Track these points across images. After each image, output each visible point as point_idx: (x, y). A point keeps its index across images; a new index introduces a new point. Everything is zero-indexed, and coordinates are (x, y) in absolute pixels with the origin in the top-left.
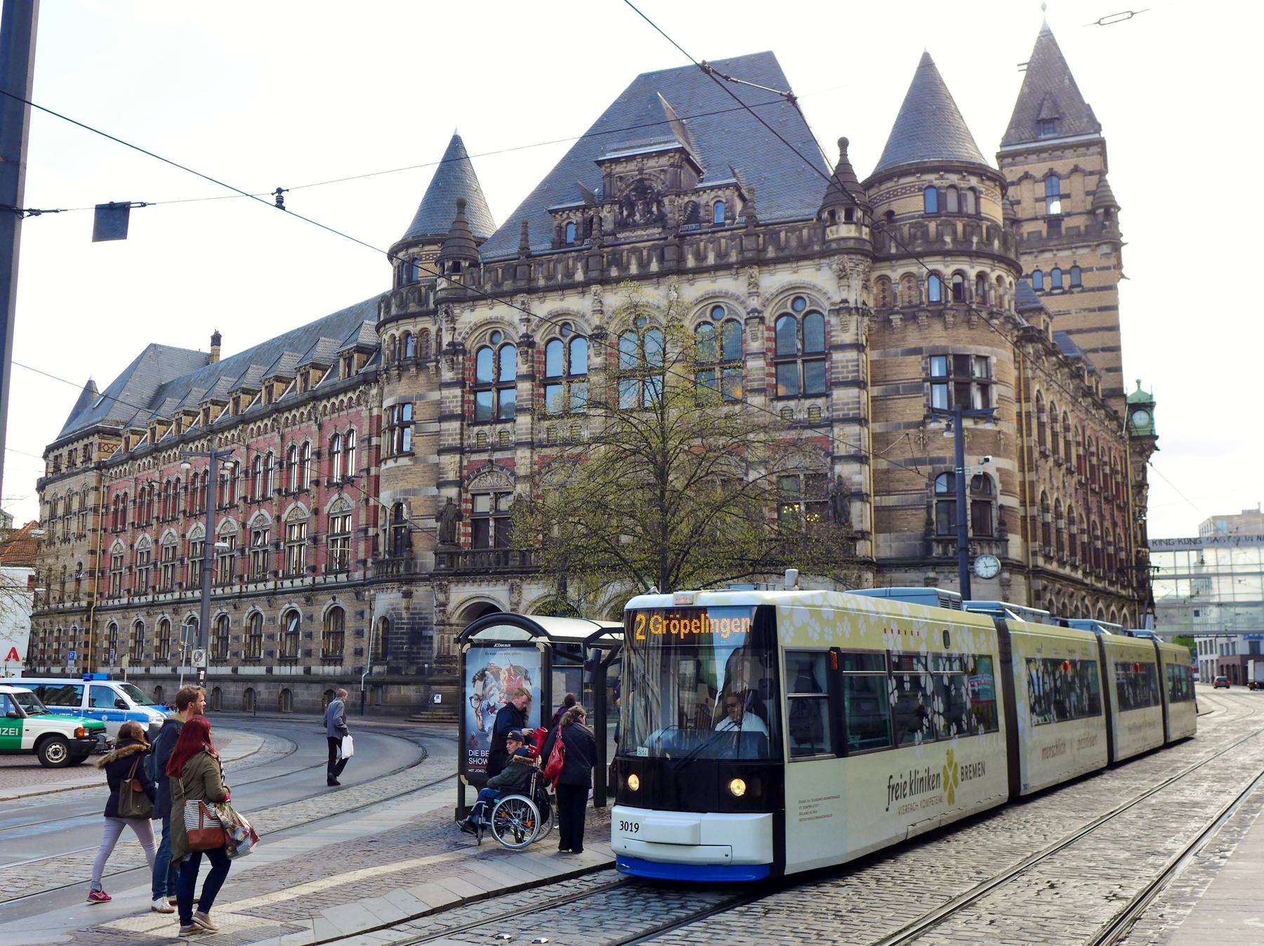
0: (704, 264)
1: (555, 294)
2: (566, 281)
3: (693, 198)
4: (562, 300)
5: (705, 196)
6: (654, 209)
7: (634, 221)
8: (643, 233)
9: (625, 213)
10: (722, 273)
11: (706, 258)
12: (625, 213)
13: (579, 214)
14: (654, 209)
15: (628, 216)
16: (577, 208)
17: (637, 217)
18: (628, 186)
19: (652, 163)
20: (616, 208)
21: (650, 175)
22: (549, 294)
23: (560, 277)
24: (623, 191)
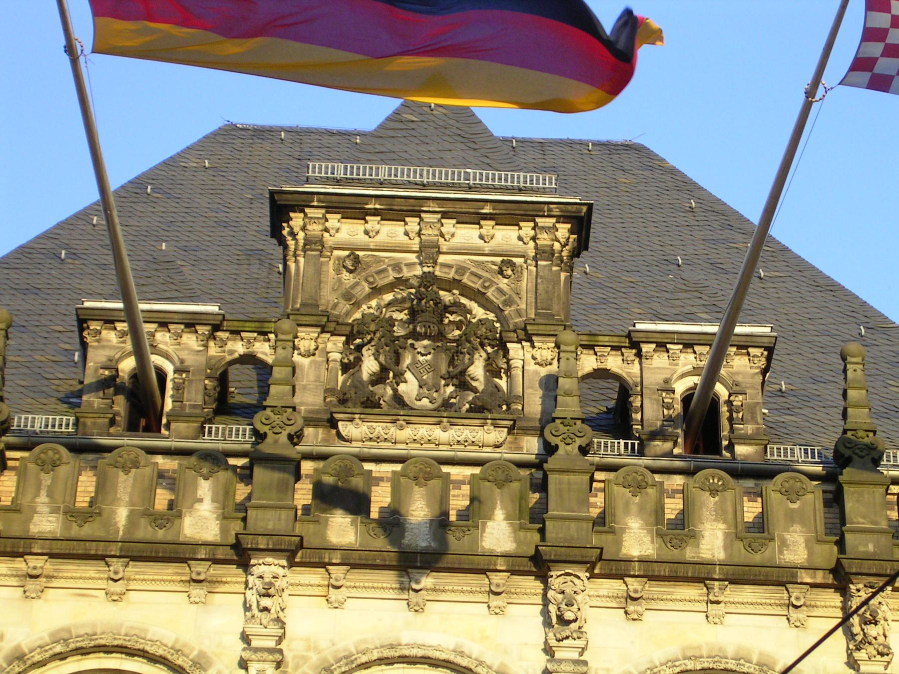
0: (689, 554)
1: (90, 570)
2: (145, 531)
3: (614, 363)
4: (115, 598)
5: (659, 361)
6: (477, 370)
7: (398, 400)
8: (437, 433)
9: (369, 365)
10: (748, 593)
11: (694, 536)
12: (369, 365)
13: (190, 340)
14: (477, 370)
15: (379, 378)
16: (191, 323)
17: (409, 388)
18: (377, 291)
19: (467, 235)
20: (335, 345)
21: (461, 270)
22: (71, 568)
23: (122, 515)
24: (357, 305)
